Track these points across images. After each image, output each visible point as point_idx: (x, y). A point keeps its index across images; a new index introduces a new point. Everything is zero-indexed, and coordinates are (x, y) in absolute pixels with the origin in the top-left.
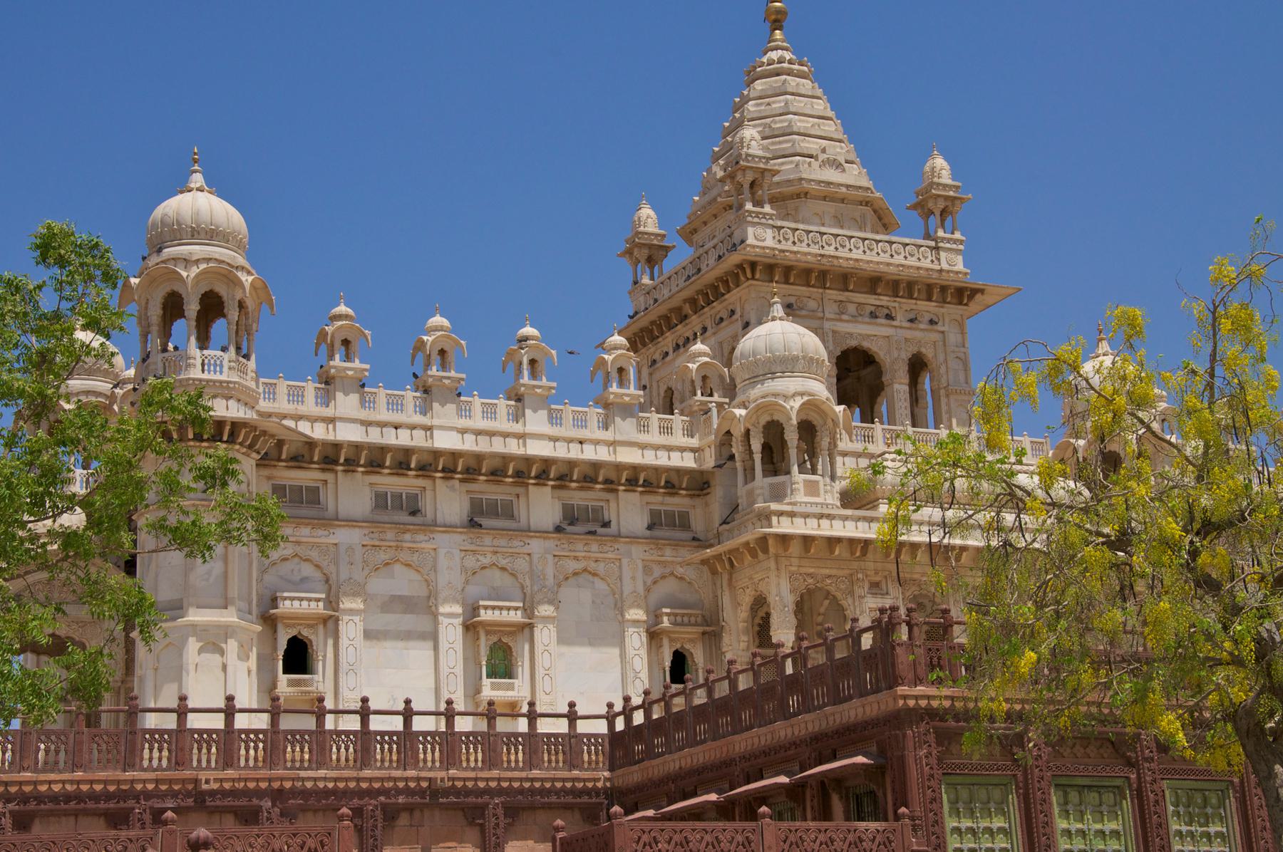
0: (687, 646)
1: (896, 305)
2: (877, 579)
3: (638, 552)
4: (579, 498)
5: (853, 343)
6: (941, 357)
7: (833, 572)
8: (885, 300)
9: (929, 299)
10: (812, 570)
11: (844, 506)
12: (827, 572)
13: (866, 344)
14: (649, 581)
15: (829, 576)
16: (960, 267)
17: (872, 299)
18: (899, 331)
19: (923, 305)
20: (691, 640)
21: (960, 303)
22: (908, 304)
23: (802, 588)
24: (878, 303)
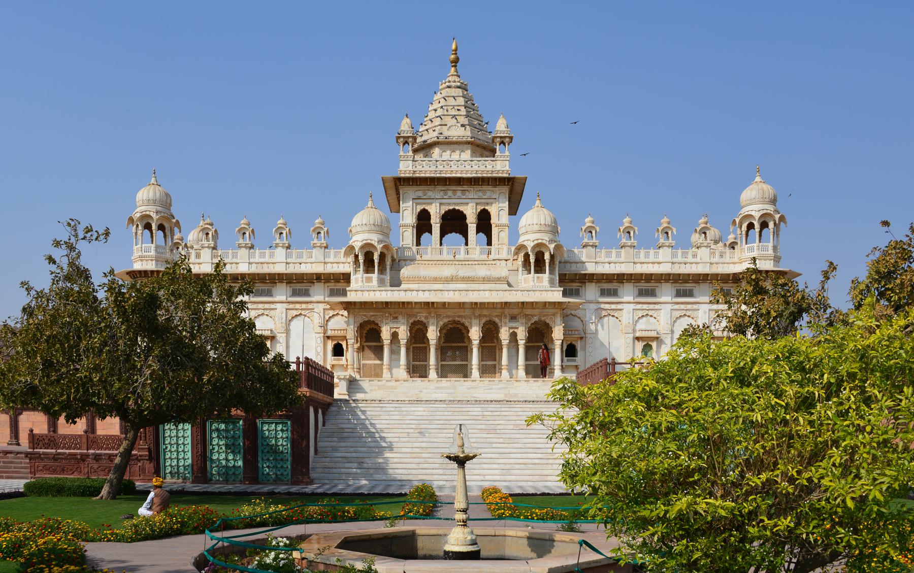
3: (322, 306)
4: (298, 286)
5: (451, 208)
8: (465, 188)
11: (391, 286)
13: (457, 208)
14: (327, 318)
16: (507, 168)
17: (459, 188)
19: (485, 188)
22: (479, 188)
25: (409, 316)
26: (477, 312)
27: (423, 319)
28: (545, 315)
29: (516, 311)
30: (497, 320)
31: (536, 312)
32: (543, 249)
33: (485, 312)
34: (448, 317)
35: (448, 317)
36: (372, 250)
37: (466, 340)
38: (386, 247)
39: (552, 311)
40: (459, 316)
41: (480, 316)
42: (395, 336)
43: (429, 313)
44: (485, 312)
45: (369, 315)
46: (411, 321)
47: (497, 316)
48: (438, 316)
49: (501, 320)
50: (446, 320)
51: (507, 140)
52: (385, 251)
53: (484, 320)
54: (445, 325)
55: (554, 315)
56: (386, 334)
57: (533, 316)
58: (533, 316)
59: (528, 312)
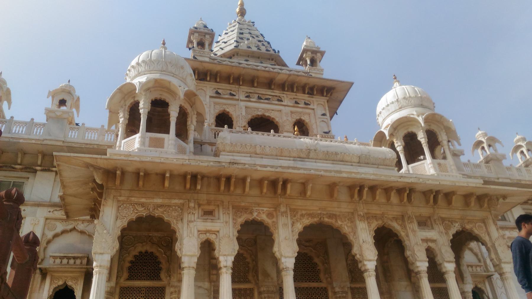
0: (70, 283)
1: (285, 95)
2: (211, 208)
6: (313, 121)
7: (166, 201)
8: (277, 93)
9: (304, 93)
10: (143, 200)
12: (159, 201)
13: (267, 114)
15: (161, 206)
17: (269, 92)
18: (287, 108)
20: (73, 278)
21: (323, 96)
22: (292, 95)
23: (134, 217)
24: (273, 94)
25: (238, 210)
26: (362, 209)
27: (264, 217)
28: (470, 222)
29: (425, 211)
30: (396, 226)
31: (455, 214)
32: (434, 127)
33: (375, 210)
34: (311, 215)
35: (311, 215)
36: (166, 97)
37: (322, 276)
38: (190, 96)
39: (479, 214)
40: (331, 216)
41: (368, 217)
42: (208, 248)
43: (276, 208)
44: (375, 210)
45: (152, 203)
46: (241, 220)
47: (395, 219)
48: (294, 212)
49: (404, 227)
50: (307, 221)
51: (319, 55)
52: (187, 106)
53: (375, 225)
54: (306, 228)
55: (484, 221)
56: (188, 250)
57: (452, 221)
58: (452, 221)
59: (444, 213)
